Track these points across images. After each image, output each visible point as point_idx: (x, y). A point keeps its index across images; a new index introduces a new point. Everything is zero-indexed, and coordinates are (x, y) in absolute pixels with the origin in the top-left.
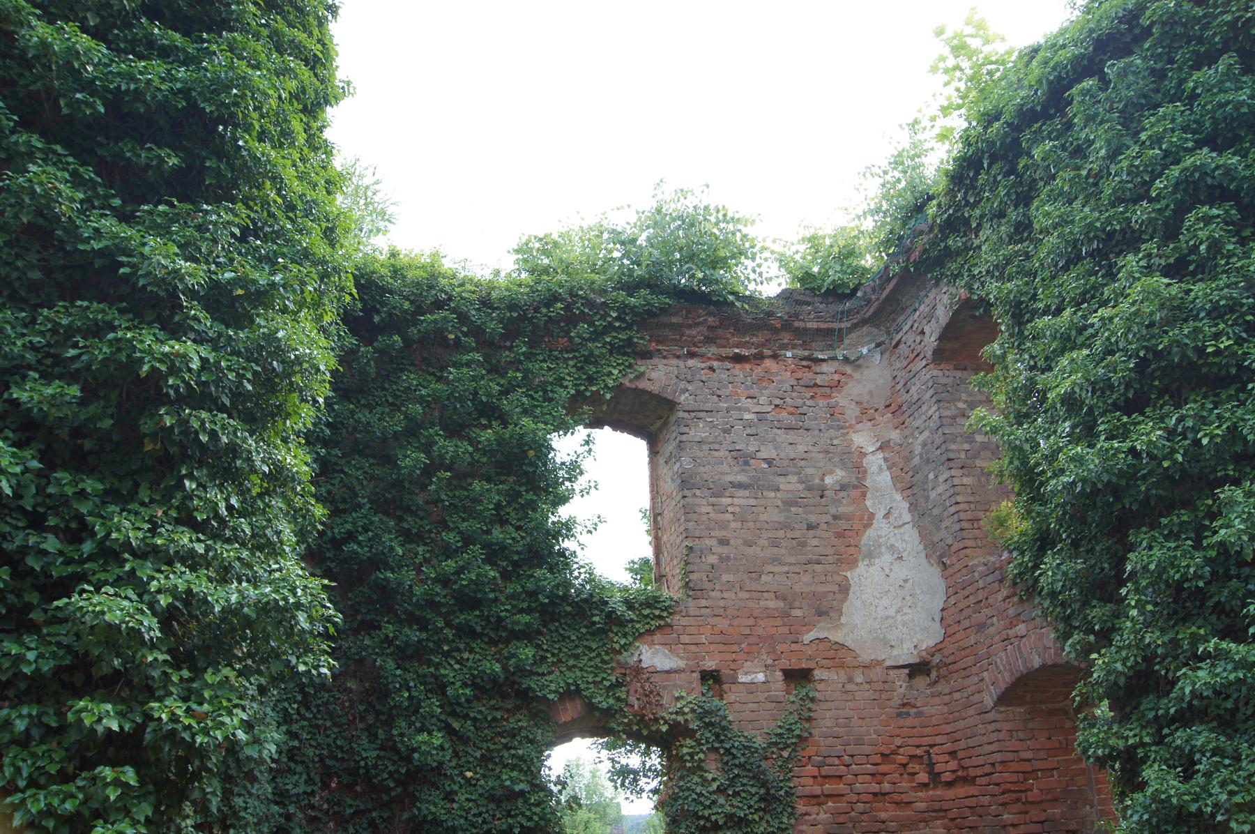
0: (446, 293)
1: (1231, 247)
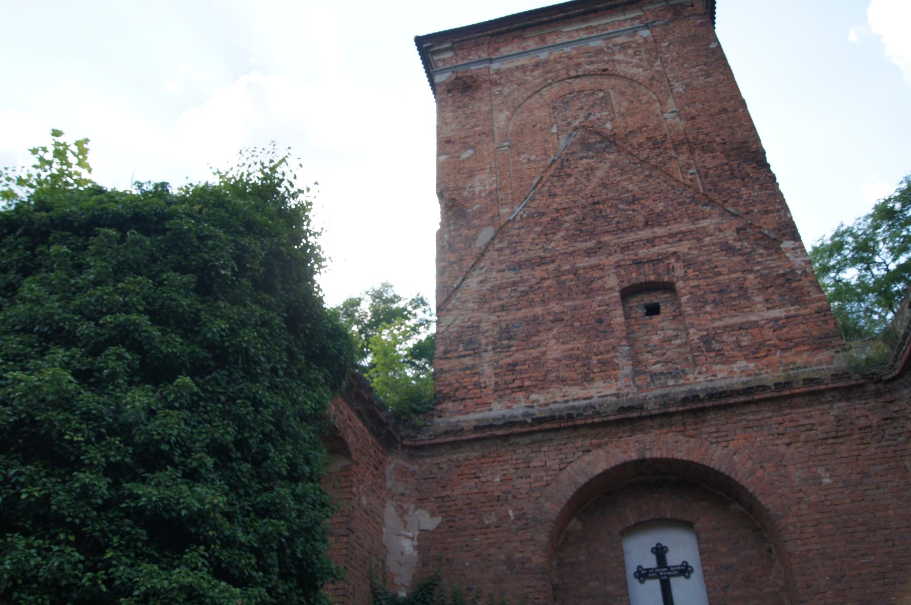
1: (121, 381)
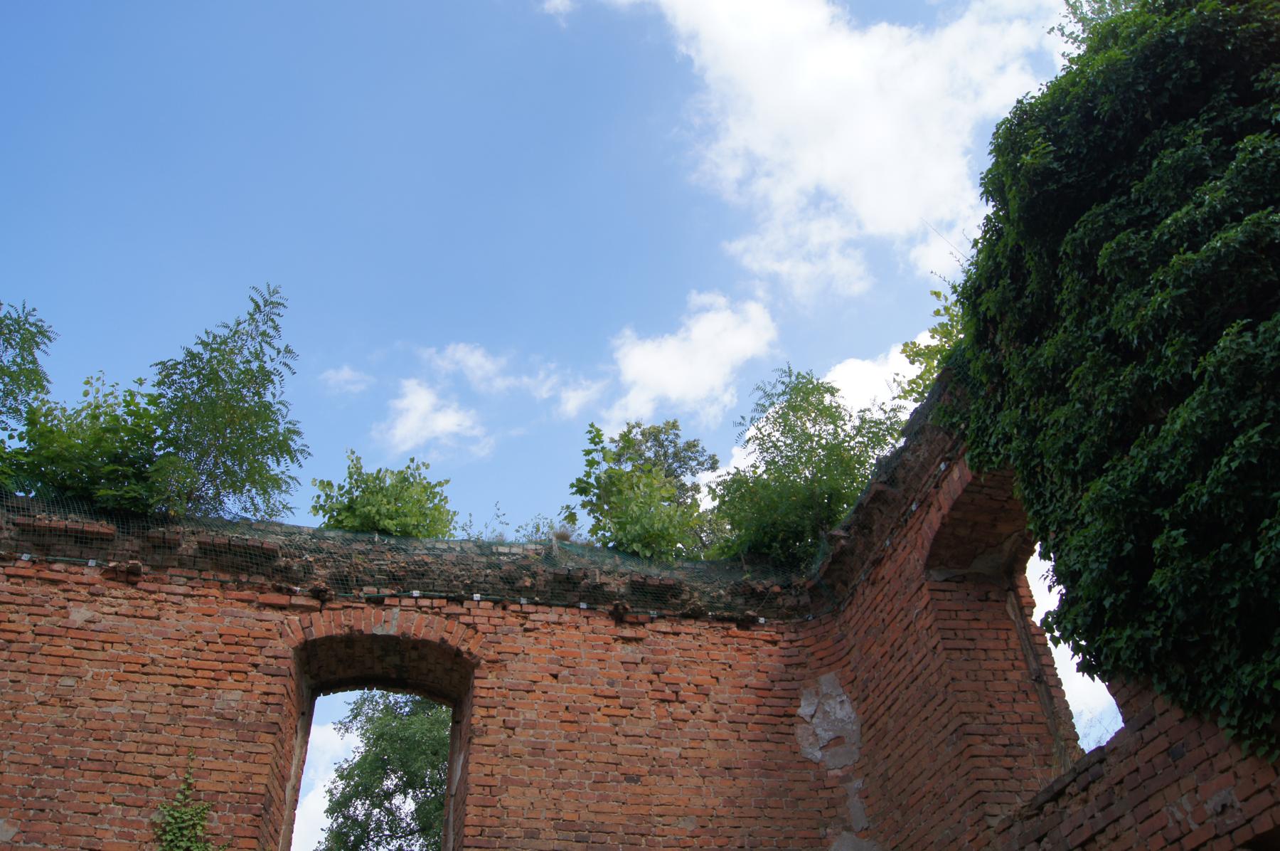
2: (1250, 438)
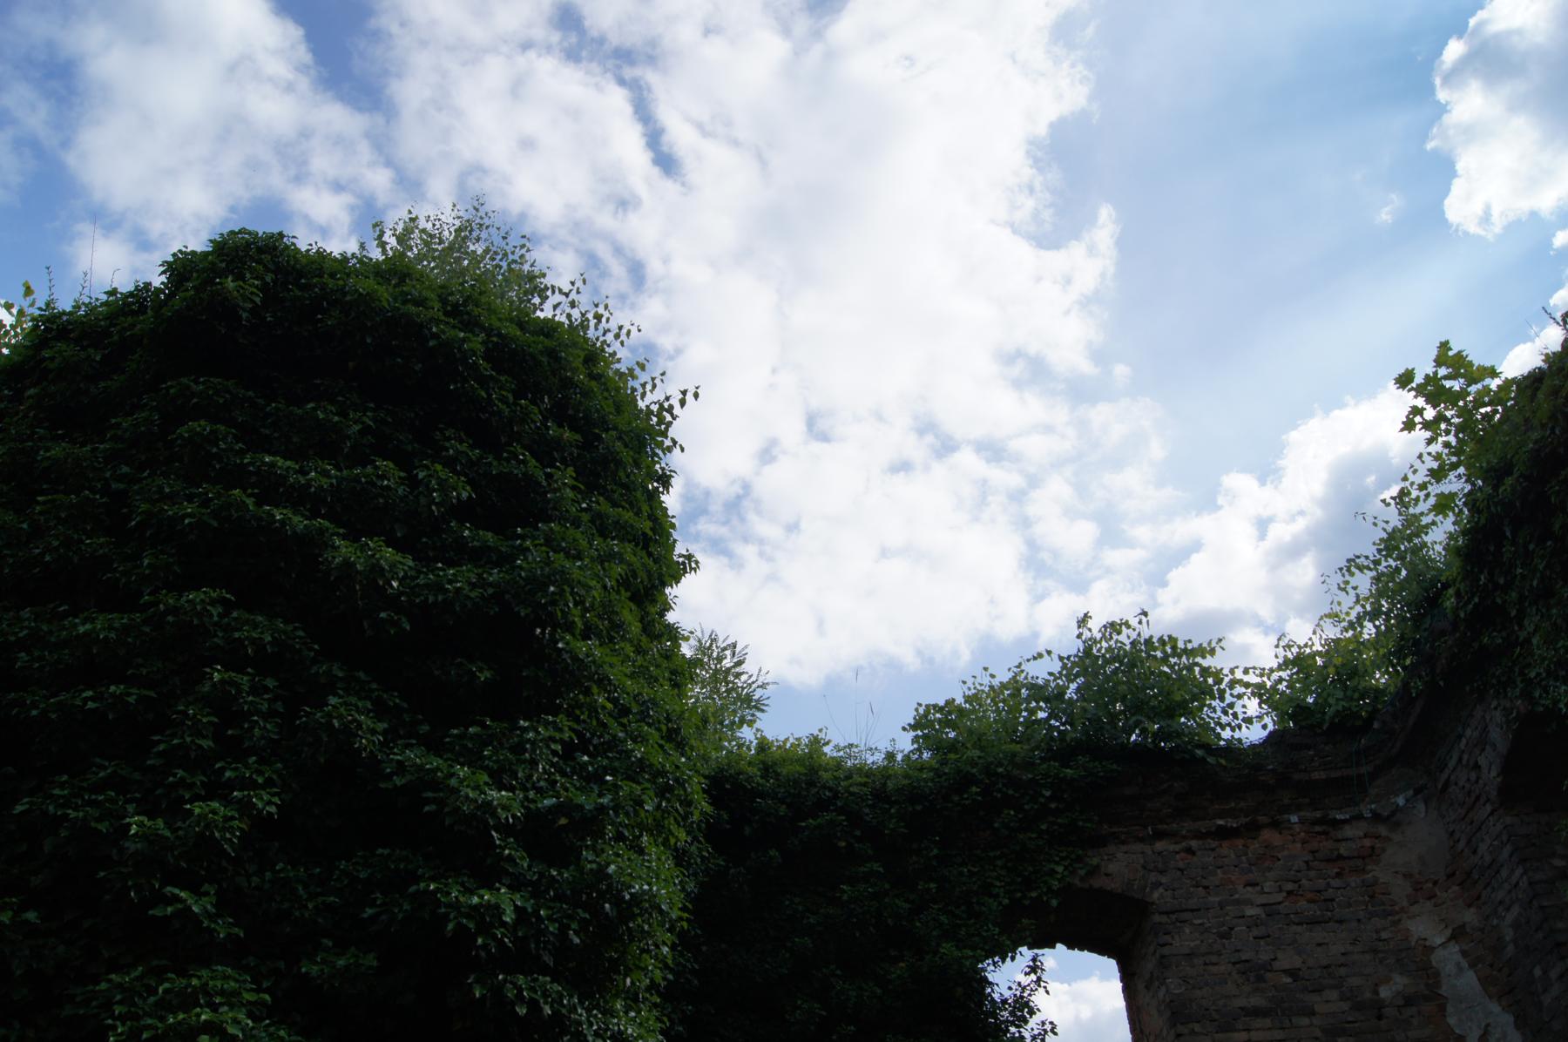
0: (830, 789)
2: (130, 694)
